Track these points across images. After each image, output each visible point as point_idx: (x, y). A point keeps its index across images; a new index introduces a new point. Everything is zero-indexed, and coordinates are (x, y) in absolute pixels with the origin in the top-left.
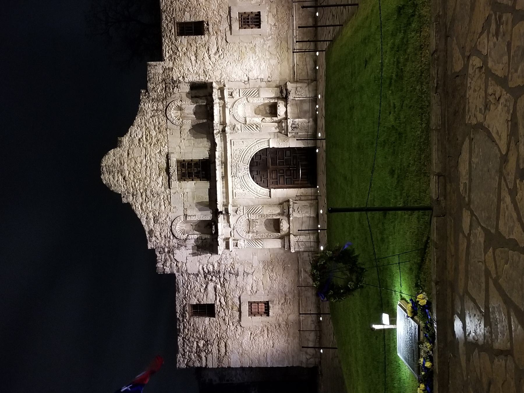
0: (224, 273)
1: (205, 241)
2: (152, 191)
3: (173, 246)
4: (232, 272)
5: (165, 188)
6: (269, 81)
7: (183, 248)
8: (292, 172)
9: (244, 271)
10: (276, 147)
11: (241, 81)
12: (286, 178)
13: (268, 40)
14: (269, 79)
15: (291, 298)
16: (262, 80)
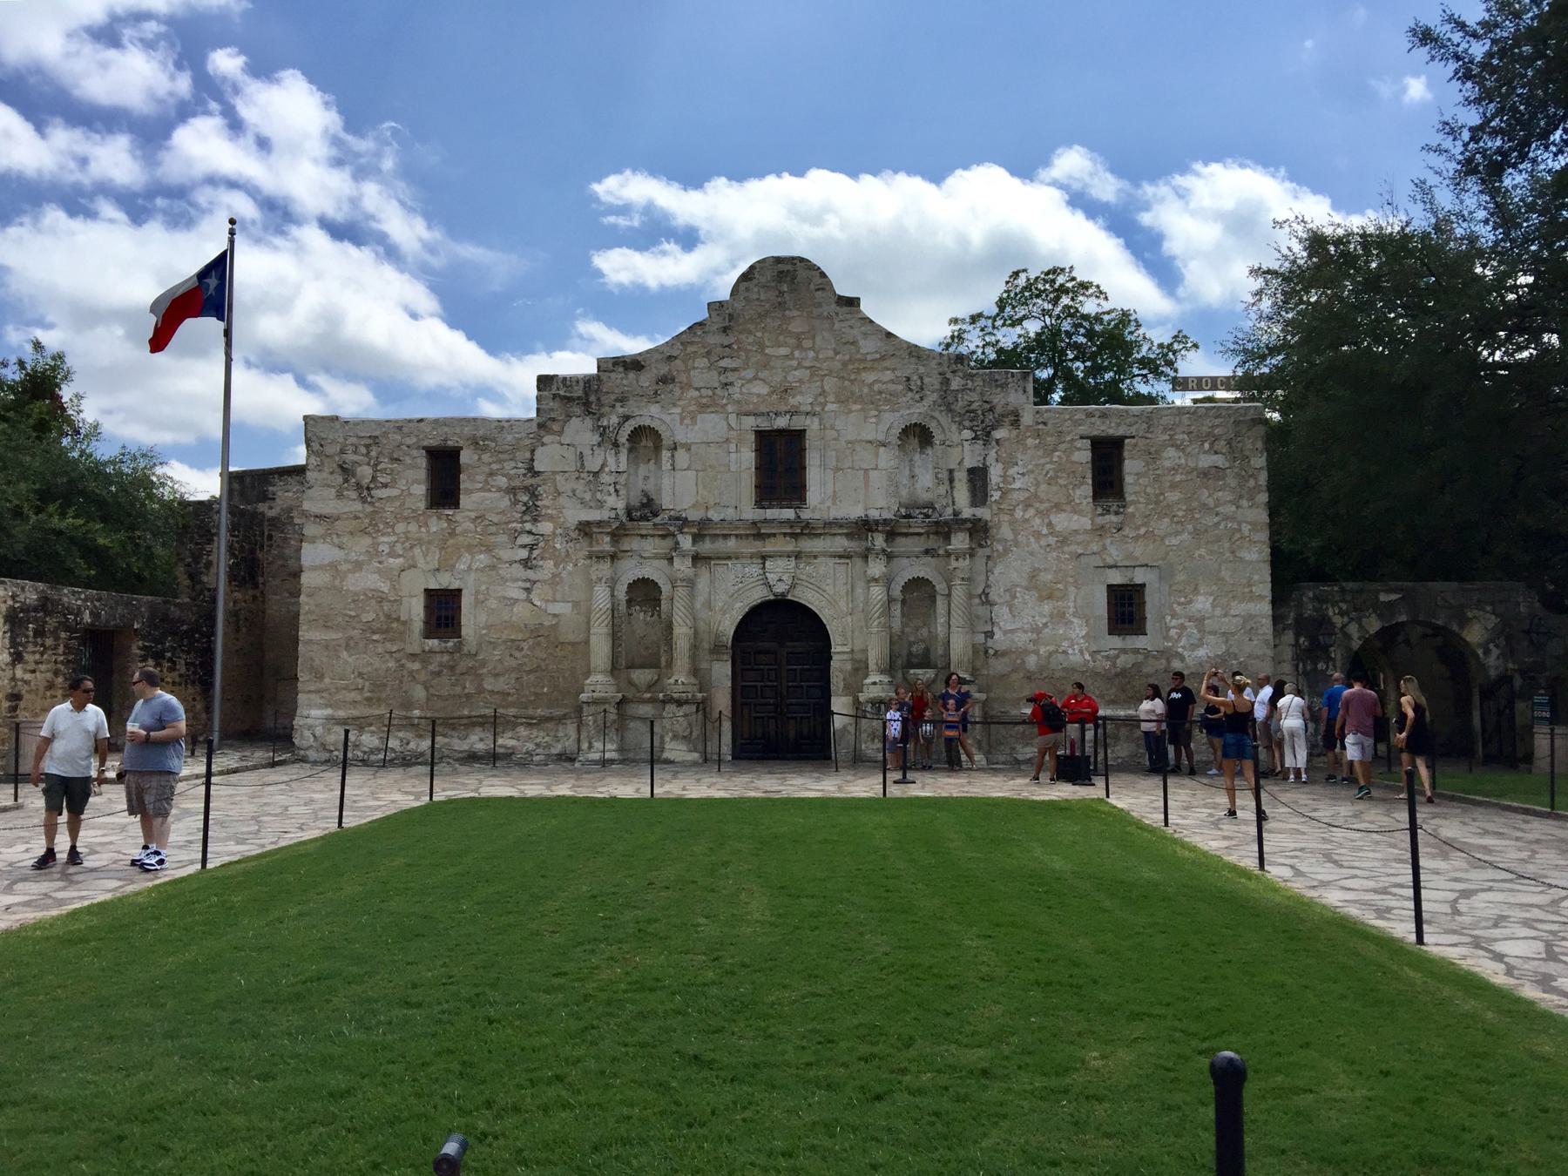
0: (533, 534)
1: (612, 489)
2: (734, 370)
3: (602, 415)
4: (535, 553)
5: (738, 402)
6: (986, 652)
7: (596, 438)
8: (772, 701)
9: (535, 582)
10: (835, 664)
11: (988, 586)
12: (756, 686)
13: (1081, 652)
14: (991, 652)
15: (466, 691)
16: (990, 635)
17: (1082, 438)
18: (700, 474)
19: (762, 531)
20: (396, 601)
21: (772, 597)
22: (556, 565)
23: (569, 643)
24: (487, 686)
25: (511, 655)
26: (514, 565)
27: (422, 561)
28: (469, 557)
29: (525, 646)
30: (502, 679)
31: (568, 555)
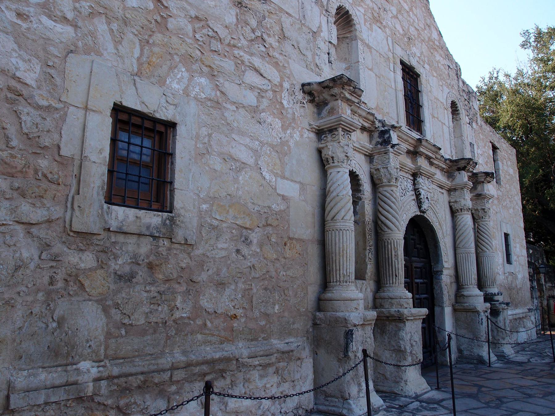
4: (265, 103)
15: (177, 315)
17: (491, 142)
18: (378, 79)
19: (421, 149)
20: (48, 108)
21: (419, 213)
22: (284, 128)
23: (297, 240)
24: (205, 303)
25: (238, 251)
26: (241, 111)
27: (111, 47)
28: (186, 75)
29: (255, 237)
30: (228, 292)
31: (294, 119)
